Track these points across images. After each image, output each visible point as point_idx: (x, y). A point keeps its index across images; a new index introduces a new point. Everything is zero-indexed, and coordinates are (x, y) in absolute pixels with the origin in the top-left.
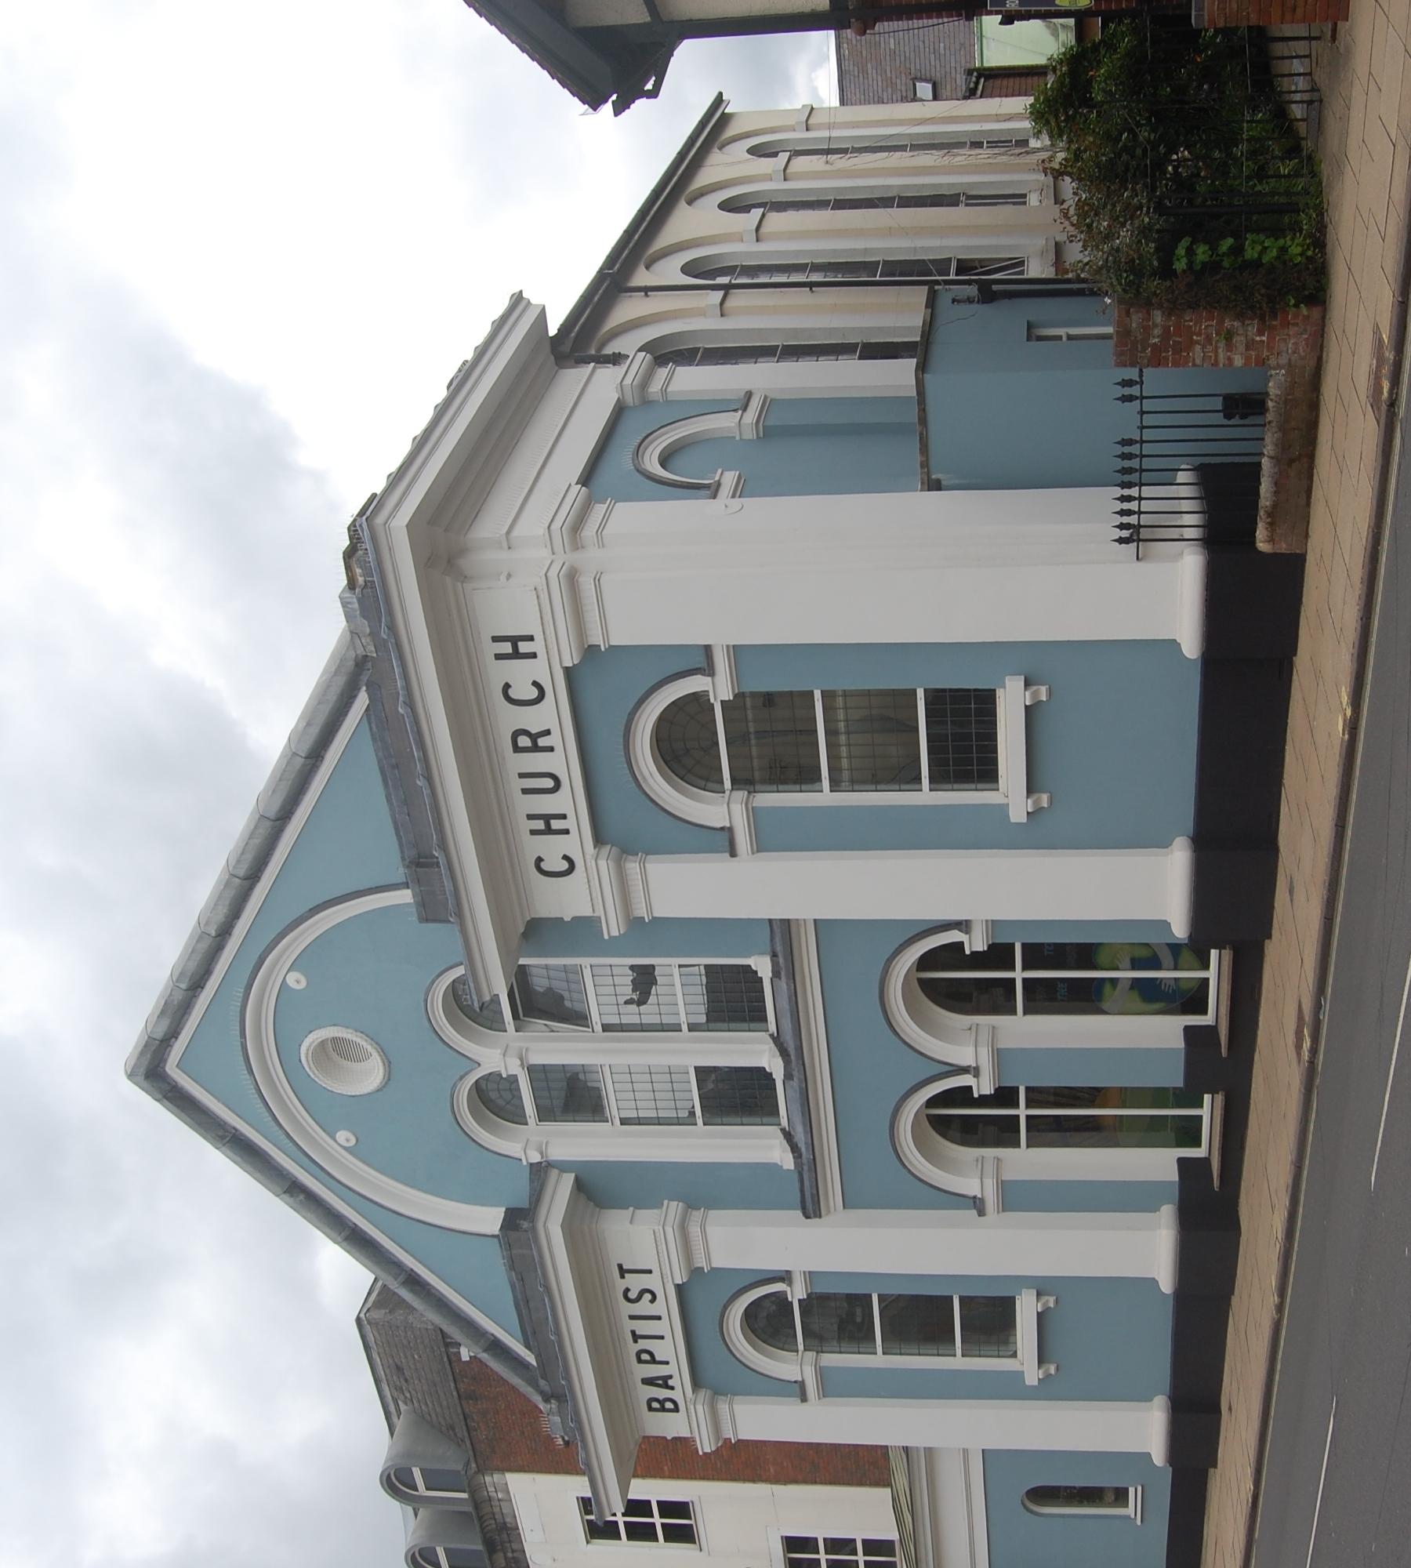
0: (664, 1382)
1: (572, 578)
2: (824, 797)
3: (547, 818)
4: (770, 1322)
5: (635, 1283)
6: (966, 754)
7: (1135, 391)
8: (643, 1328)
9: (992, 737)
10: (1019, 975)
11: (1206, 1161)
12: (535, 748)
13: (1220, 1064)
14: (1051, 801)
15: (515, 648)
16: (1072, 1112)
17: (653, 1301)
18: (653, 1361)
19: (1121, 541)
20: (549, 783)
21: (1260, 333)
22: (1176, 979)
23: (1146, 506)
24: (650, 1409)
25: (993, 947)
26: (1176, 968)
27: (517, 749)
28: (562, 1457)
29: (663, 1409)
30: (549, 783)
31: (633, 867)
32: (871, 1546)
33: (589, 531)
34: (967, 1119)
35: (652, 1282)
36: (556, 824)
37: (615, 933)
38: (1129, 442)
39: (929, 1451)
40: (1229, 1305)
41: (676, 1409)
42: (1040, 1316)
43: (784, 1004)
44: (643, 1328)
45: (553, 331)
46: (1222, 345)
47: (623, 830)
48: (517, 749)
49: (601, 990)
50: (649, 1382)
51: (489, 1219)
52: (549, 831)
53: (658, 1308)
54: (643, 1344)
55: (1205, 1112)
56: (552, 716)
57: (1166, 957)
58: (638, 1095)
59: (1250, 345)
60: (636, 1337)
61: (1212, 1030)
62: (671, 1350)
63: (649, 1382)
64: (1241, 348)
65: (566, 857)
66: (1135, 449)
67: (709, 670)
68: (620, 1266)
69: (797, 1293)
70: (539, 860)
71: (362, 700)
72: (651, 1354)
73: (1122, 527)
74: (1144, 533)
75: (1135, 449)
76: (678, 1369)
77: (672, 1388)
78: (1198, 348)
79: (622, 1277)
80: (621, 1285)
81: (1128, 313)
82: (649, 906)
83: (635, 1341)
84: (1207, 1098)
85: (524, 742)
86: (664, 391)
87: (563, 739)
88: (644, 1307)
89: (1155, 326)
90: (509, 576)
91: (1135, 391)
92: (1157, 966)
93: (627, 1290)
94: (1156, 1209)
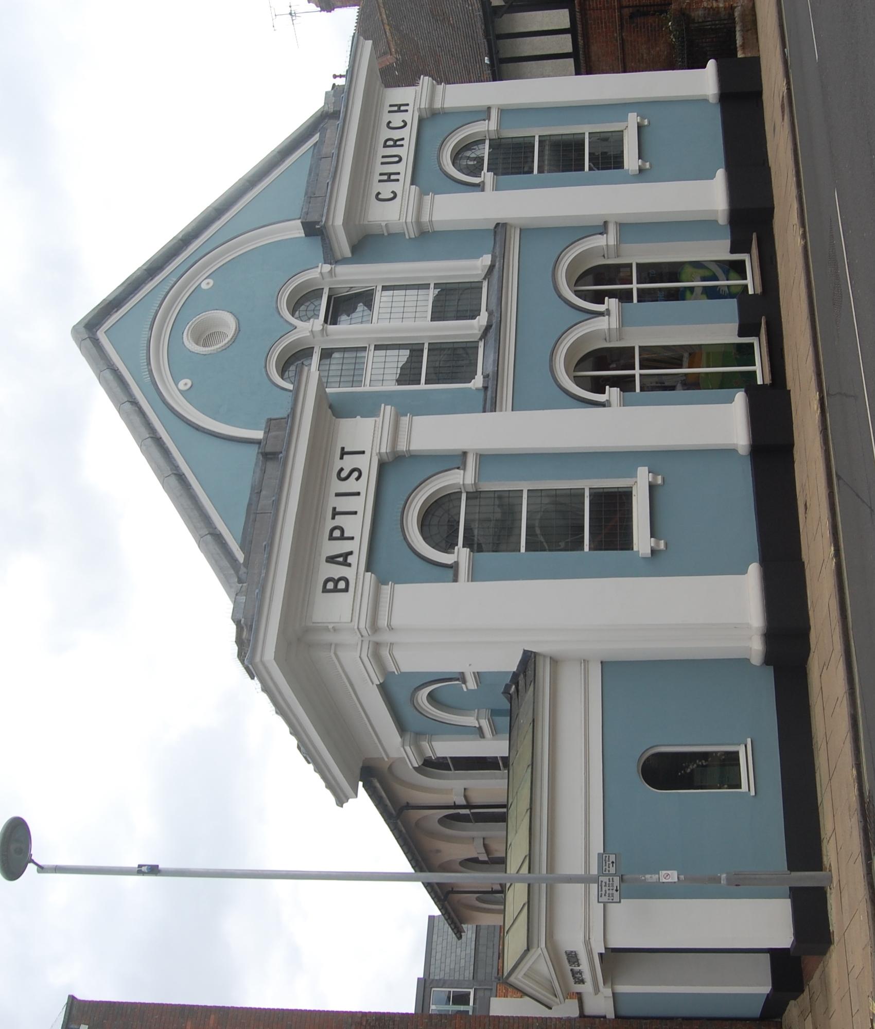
3: (390, 174)
4: (439, 521)
5: (349, 463)
8: (344, 504)
12: (395, 145)
13: (761, 314)
18: (342, 537)
20: (397, 159)
22: (729, 286)
24: (325, 590)
26: (727, 280)
29: (336, 590)
30: (397, 159)
41: (346, 590)
42: (652, 487)
43: (494, 300)
44: (344, 504)
49: (382, 305)
50: (331, 560)
52: (389, 180)
53: (360, 486)
54: (340, 520)
60: (335, 513)
62: (358, 527)
63: (331, 560)
65: (393, 192)
68: (343, 449)
71: (316, 138)
76: (358, 548)
77: (349, 565)
79: (342, 458)
80: (338, 464)
82: (431, 215)
83: (333, 518)
85: (390, 143)
88: (351, 485)
93: (342, 469)
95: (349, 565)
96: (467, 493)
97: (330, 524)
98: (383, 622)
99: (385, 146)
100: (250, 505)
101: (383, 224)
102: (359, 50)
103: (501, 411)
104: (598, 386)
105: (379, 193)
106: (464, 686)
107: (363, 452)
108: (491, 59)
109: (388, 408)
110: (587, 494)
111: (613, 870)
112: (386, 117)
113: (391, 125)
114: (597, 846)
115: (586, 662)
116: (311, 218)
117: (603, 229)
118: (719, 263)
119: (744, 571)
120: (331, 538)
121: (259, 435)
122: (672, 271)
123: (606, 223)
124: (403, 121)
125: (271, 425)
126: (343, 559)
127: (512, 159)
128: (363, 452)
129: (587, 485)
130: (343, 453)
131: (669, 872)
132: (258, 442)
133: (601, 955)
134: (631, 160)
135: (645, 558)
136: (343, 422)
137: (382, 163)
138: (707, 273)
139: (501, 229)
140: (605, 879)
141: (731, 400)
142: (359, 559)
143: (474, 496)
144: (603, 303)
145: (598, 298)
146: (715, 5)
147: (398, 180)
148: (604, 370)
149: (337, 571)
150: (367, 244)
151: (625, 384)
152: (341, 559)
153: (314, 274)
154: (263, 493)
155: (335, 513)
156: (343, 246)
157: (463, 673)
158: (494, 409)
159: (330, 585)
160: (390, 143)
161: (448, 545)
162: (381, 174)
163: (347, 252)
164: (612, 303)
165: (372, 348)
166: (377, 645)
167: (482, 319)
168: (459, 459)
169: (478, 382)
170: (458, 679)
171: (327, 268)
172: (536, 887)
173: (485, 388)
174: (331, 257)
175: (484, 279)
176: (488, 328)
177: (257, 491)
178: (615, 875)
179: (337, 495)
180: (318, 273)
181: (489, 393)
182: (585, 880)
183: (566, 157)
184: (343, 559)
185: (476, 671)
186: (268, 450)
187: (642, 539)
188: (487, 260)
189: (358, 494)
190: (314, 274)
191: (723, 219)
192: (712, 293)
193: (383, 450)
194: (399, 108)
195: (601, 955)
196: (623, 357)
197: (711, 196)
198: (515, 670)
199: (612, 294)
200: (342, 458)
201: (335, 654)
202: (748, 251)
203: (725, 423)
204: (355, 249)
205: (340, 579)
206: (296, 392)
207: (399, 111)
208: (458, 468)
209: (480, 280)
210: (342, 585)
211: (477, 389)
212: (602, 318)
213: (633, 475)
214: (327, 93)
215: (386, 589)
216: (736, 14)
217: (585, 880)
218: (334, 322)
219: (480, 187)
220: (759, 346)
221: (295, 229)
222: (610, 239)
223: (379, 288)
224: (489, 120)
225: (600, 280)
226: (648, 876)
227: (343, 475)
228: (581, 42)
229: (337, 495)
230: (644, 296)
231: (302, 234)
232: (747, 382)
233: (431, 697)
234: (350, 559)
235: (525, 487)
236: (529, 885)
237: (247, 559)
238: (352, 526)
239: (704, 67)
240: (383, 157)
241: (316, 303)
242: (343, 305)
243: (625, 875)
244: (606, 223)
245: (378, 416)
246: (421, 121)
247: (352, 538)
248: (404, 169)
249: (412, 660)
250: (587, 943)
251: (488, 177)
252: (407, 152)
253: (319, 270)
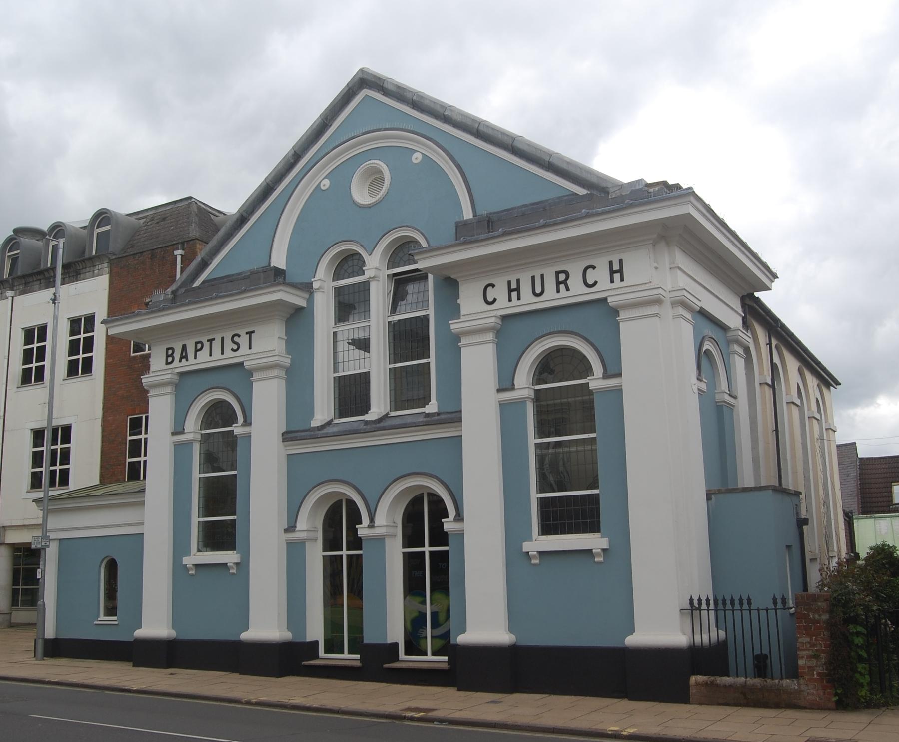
0: (184, 356)
1: (658, 302)
2: (533, 441)
3: (518, 290)
4: (219, 414)
6: (556, 518)
7: (779, 605)
9: (570, 532)
10: (427, 549)
11: (317, 657)
12: (558, 283)
14: (535, 565)
15: (616, 272)
16: (346, 580)
17: (233, 350)
18: (197, 351)
19: (691, 600)
20: (538, 291)
21: (818, 674)
23: (737, 614)
24: (168, 349)
25: (446, 534)
26: (432, 637)
27: (558, 273)
28: (121, 304)
29: (168, 356)
30: (538, 291)
31: (490, 336)
32: (65, 474)
33: (681, 311)
34: (340, 523)
35: (244, 349)
36: (514, 294)
37: (452, 327)
38: (749, 602)
39: (143, 503)
40: (236, 672)
41: (167, 363)
42: (225, 565)
43: (409, 420)
44: (217, 345)
45: (756, 294)
46: (810, 653)
47: (510, 332)
48: (558, 273)
50: (184, 348)
51: (279, 260)
53: (228, 353)
54: (207, 345)
55: (346, 655)
56: (577, 291)
57: (440, 631)
59: (811, 668)
60: (211, 341)
61: (396, 658)
62: (204, 360)
63: (184, 348)
64: (809, 664)
65: (495, 300)
66: (745, 606)
67: (606, 376)
68: (253, 332)
69: (237, 429)
70: (493, 286)
73: (700, 600)
74: (696, 613)
75: (745, 606)
76: (193, 363)
77: (180, 361)
78: (808, 639)
79: (247, 333)
80: (242, 332)
81: (826, 600)
84: (358, 656)
85: (562, 277)
86: (735, 352)
87: (564, 298)
88: (229, 345)
89: (820, 615)
90: (656, 268)
91: (779, 605)
92: (434, 626)
93: (239, 336)
94: (289, 629)
97: (204, 340)
102: (672, 202)
103: (285, 446)
130: (250, 333)
138: (442, 617)
149: (177, 356)
220: (348, 657)
234: (184, 360)
238: (203, 355)
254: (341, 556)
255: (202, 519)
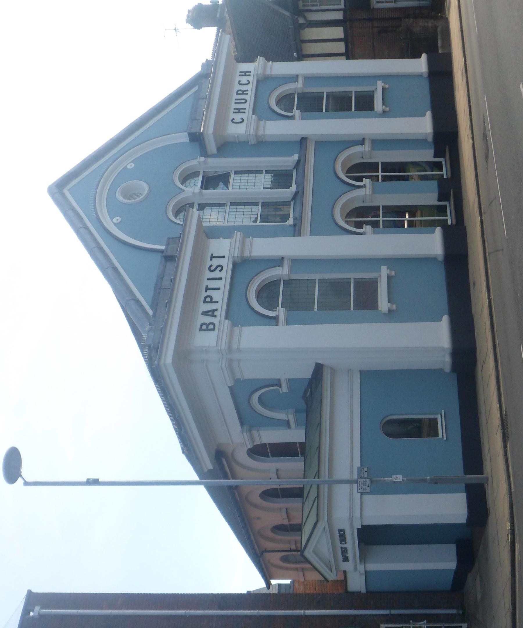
3: (240, 109)
5: (215, 262)
12: (243, 94)
13: (451, 189)
18: (211, 302)
20: (244, 101)
24: (201, 329)
29: (207, 329)
30: (244, 101)
35: (223, 262)
41: (213, 329)
50: (205, 313)
52: (239, 112)
53: (222, 274)
54: (210, 293)
58: (237, 216)
60: (207, 289)
62: (220, 297)
63: (205, 313)
72: (211, 298)
76: (221, 307)
77: (215, 316)
79: (211, 260)
80: (209, 263)
83: (206, 291)
85: (240, 92)
93: (211, 266)
95: (215, 316)
96: (284, 280)
98: (235, 346)
99: (237, 94)
100: (156, 285)
101: (236, 136)
104: (359, 225)
105: (233, 119)
106: (280, 389)
107: (224, 257)
108: (297, 55)
109: (239, 233)
110: (352, 281)
111: (366, 476)
112: (238, 78)
113: (241, 83)
114: (357, 463)
115: (350, 371)
116: (193, 131)
117: (362, 142)
118: (428, 163)
119: (440, 320)
120: (205, 302)
121: (163, 247)
122: (402, 166)
123: (364, 139)
124: (248, 81)
125: (170, 241)
126: (212, 313)
127: (311, 104)
128: (224, 257)
129: (352, 276)
130: (212, 257)
131: (398, 476)
132: (162, 251)
133: (358, 529)
134: (378, 105)
135: (384, 314)
136: (212, 241)
137: (236, 103)
139: (303, 141)
140: (362, 480)
141: (433, 232)
142: (221, 313)
143: (288, 283)
144: (362, 181)
145: (360, 179)
146: (426, 24)
147: (245, 112)
148: (362, 216)
149: (208, 319)
150: (226, 147)
151: (375, 225)
152: (210, 313)
153: (194, 162)
154: (165, 278)
155: (207, 289)
156: (212, 146)
157: (279, 380)
158: (299, 235)
159: (204, 327)
160: (240, 92)
161: (272, 307)
162: (235, 109)
163: (215, 151)
164: (367, 182)
165: (229, 204)
166: (231, 360)
167: (294, 188)
168: (279, 262)
169: (291, 221)
170: (276, 385)
171: (202, 159)
172: (322, 486)
173: (295, 225)
174: (205, 153)
175: (294, 168)
176: (296, 193)
177: (161, 278)
178: (367, 478)
179: (209, 279)
180: (198, 162)
181: (297, 227)
182: (350, 482)
183: (341, 104)
184: (212, 313)
185: (288, 377)
186: (169, 253)
187: (383, 304)
188: (296, 157)
189: (221, 279)
190: (194, 162)
191: (430, 139)
192: (423, 178)
193: (236, 255)
194: (245, 74)
195: (358, 529)
196: (373, 210)
197: (424, 125)
198: (310, 376)
199: (367, 177)
200: (211, 260)
201: (207, 366)
202: (444, 156)
203: (431, 243)
204: (219, 149)
205: (210, 324)
206: (184, 226)
207: (245, 75)
208: (279, 266)
209: (291, 169)
210: (211, 327)
211: (290, 226)
212: (361, 189)
213: (379, 270)
214: (203, 64)
215: (237, 329)
216: (439, 29)
217: (350, 482)
218: (206, 189)
219: (292, 118)
221: (184, 138)
222: (367, 147)
223: (233, 172)
224: (297, 82)
225: (361, 170)
226: (386, 479)
227: (212, 268)
228: (350, 46)
229: (209, 279)
230: (385, 179)
231: (187, 140)
232: (444, 225)
233: (260, 399)
234: (216, 313)
235: (317, 277)
236: (318, 486)
237: (154, 315)
238: (216, 295)
239: (420, 57)
240: (236, 100)
241: (196, 179)
242: (211, 181)
243: (373, 480)
244: (364, 139)
245: (232, 237)
246: (258, 82)
247: (217, 302)
248: (248, 107)
249: (252, 372)
250: (351, 518)
251: (297, 113)
252: (250, 97)
253: (198, 160)
254: (383, 221)
255: (352, 281)
